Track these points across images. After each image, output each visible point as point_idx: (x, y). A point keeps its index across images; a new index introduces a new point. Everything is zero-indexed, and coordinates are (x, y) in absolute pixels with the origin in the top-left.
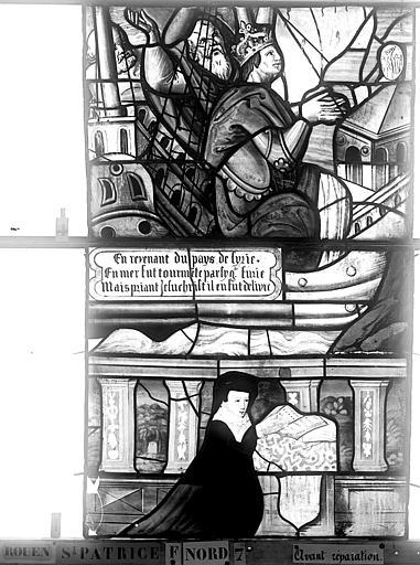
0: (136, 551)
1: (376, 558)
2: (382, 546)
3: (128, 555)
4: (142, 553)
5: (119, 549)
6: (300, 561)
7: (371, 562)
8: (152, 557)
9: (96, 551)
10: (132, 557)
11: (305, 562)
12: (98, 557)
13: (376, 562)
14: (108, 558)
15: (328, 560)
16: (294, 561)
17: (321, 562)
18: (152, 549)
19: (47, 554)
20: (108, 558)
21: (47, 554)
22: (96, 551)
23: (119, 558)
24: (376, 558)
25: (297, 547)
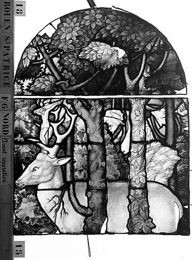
0: (6, 75)
1: (4, 181)
3: (7, 71)
5: (9, 67)
6: (2, 141)
7: (2, 179)
8: (4, 84)
9: (8, 54)
10: (4, 73)
11: (2, 143)
12: (4, 55)
14: (4, 60)
15: (3, 155)
16: (2, 138)
17: (2, 152)
18: (9, 84)
20: (4, 60)
22: (8, 54)
23: (4, 66)
24: (4, 181)
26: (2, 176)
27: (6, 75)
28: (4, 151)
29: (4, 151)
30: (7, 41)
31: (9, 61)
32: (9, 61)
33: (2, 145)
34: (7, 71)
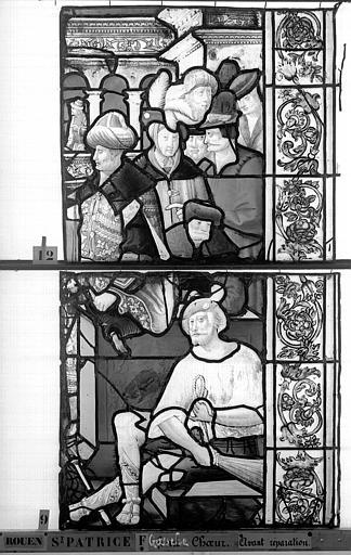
0: (112, 544)
2: (310, 534)
3: (106, 543)
4: (117, 542)
7: (302, 547)
13: (305, 547)
15: (267, 544)
17: (261, 547)
18: (125, 538)
19: (40, 543)
21: (40, 543)
22: (79, 541)
25: (241, 536)
26: (298, 547)
27: (112, 544)
28: (261, 543)
29: (261, 543)
30: (59, 541)
31: (89, 539)
32: (89, 539)
33: (251, 547)
34: (106, 543)
